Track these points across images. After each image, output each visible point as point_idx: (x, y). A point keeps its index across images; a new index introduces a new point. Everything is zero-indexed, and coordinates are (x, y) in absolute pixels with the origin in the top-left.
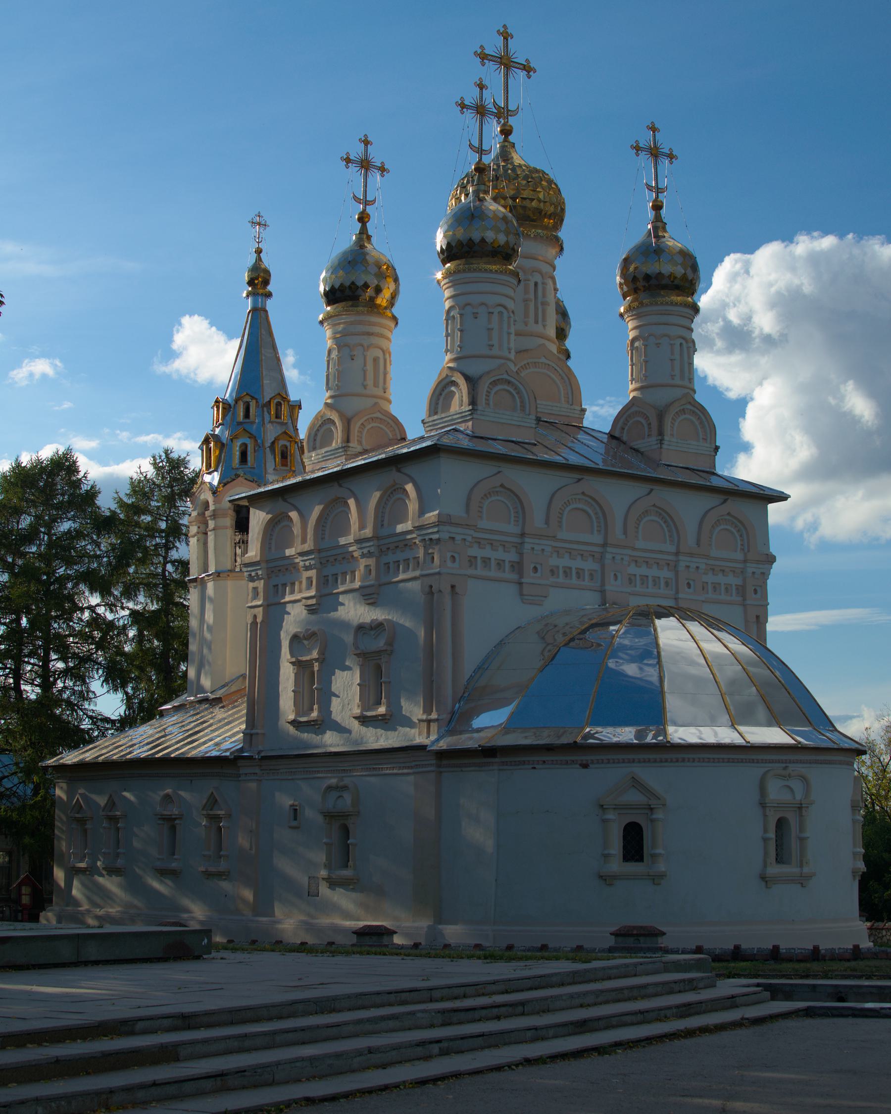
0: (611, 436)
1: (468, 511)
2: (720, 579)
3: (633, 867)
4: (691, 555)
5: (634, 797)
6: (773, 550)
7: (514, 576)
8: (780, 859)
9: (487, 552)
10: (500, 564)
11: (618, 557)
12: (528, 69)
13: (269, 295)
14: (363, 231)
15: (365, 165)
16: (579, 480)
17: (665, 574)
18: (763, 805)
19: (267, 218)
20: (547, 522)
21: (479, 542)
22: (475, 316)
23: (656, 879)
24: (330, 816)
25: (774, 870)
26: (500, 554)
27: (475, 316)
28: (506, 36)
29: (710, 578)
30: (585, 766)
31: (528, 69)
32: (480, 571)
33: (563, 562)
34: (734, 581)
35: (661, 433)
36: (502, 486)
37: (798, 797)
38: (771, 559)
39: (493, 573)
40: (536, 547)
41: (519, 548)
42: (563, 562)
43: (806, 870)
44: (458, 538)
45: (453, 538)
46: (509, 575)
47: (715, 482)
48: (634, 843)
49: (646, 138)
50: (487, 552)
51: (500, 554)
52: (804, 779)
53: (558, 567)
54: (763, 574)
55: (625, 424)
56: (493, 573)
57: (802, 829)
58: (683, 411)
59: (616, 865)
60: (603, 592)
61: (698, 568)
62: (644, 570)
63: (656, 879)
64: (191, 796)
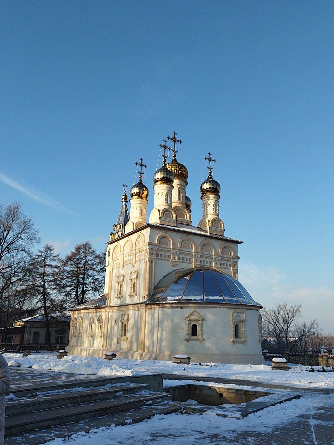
11: (197, 256)
12: (180, 142)
14: (141, 180)
16: (187, 236)
19: (127, 185)
28: (175, 134)
30: (181, 308)
31: (180, 142)
36: (166, 236)
40: (175, 252)
44: (154, 249)
45: (152, 249)
47: (224, 238)
48: (194, 330)
49: (208, 156)
53: (181, 257)
54: (236, 261)
55: (201, 224)
61: (219, 259)
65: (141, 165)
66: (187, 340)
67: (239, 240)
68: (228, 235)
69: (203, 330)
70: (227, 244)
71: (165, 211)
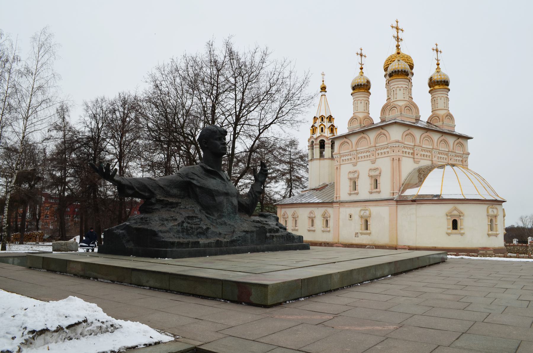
0: (427, 122)
1: (402, 139)
2: (457, 158)
3: (455, 231)
4: (452, 152)
5: (455, 213)
6: (469, 151)
7: (412, 156)
8: (491, 229)
9: (406, 150)
10: (409, 153)
13: (326, 92)
15: (361, 55)
17: (445, 157)
18: (488, 216)
20: (420, 142)
21: (404, 147)
22: (400, 90)
23: (462, 234)
24: (362, 217)
25: (490, 232)
26: (409, 151)
27: (400, 90)
29: (455, 158)
32: (404, 155)
33: (423, 153)
34: (460, 159)
35: (443, 121)
37: (495, 213)
38: (469, 154)
39: (407, 155)
41: (413, 149)
42: (423, 153)
43: (497, 233)
46: (411, 156)
47: (454, 133)
50: (406, 150)
51: (409, 151)
52: (496, 208)
56: (407, 155)
57: (496, 222)
58: (447, 116)
59: (451, 231)
60: (432, 161)
62: (441, 156)
63: (462, 234)
64: (318, 212)
65: (361, 55)
66: (449, 234)
67: (469, 135)
68: (458, 130)
69: (465, 224)
70: (460, 140)
71: (406, 107)
